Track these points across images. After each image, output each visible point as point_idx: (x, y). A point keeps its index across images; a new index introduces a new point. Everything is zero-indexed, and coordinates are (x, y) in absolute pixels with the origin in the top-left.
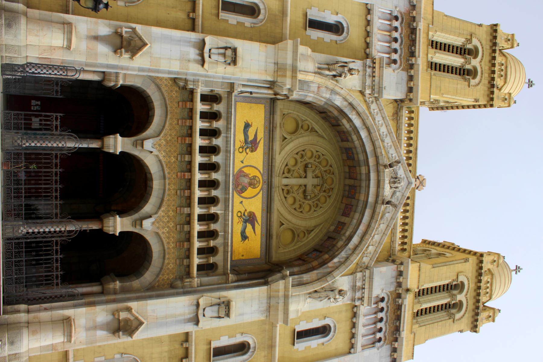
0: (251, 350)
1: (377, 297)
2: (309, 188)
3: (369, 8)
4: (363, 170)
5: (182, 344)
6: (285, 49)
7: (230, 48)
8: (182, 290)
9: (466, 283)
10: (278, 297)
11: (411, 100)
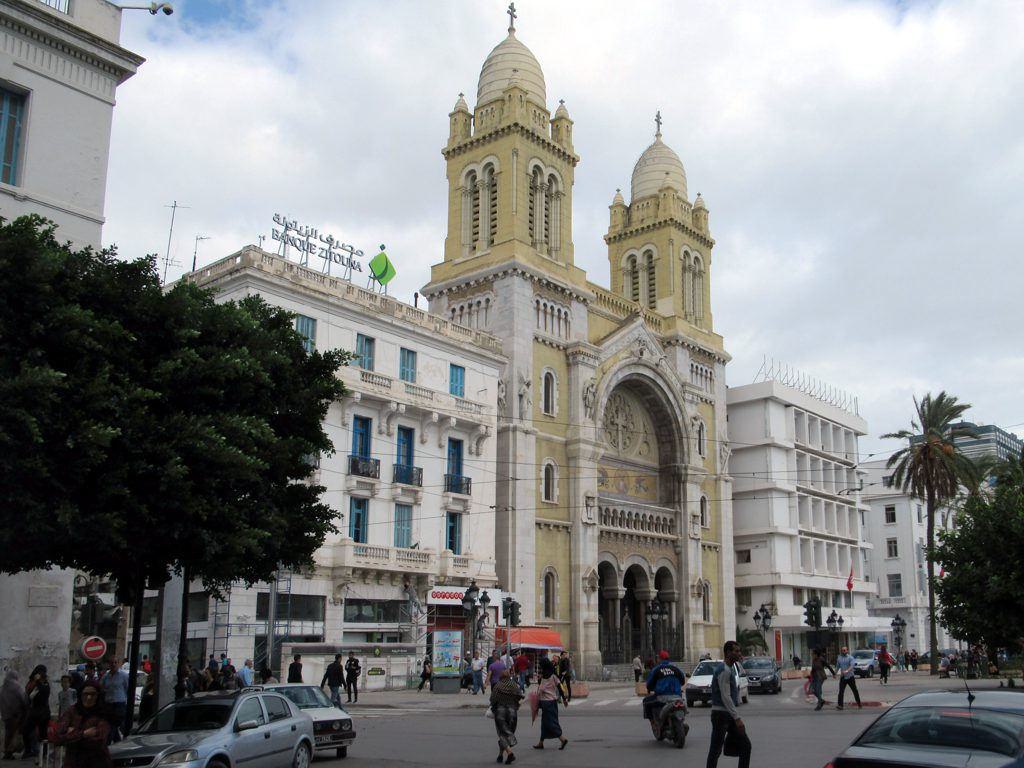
2: (624, 423)
4: (634, 377)
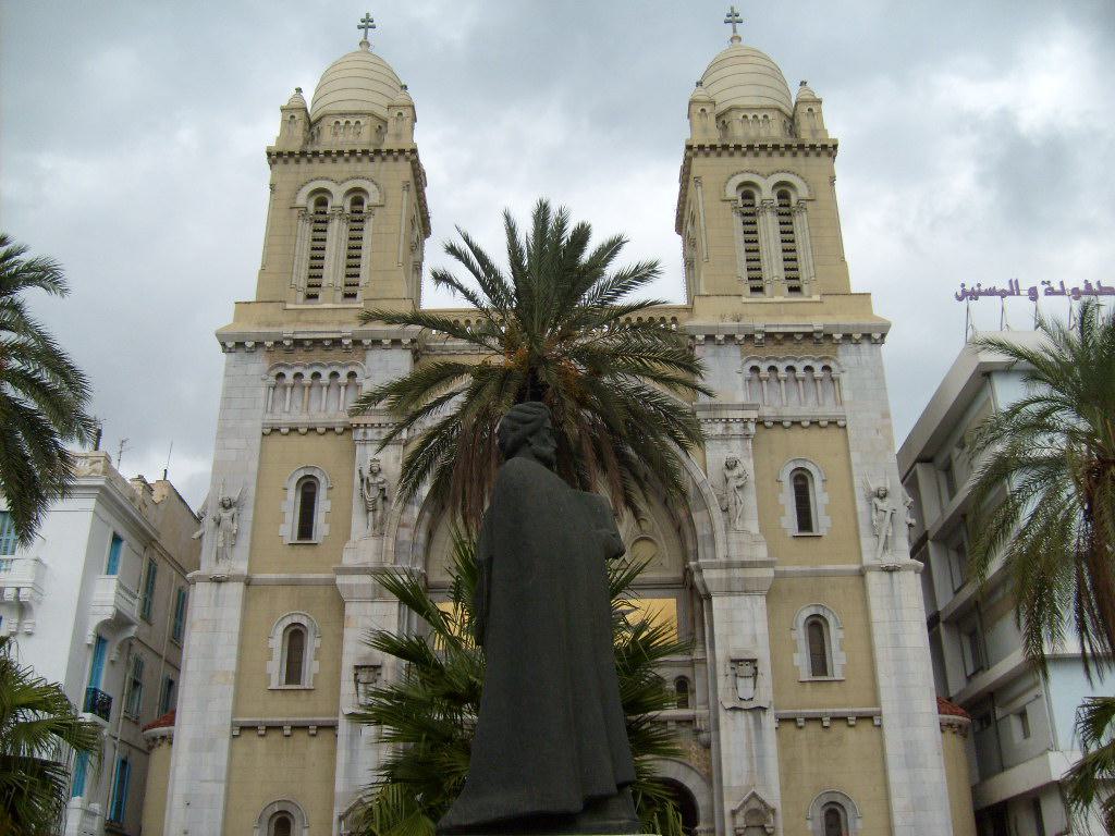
0: (821, 613)
1: (749, 381)
3: (268, 431)
5: (801, 727)
6: (349, 586)
7: (356, 675)
8: (712, 734)
9: (740, 179)
10: (729, 580)
11: (413, 341)
